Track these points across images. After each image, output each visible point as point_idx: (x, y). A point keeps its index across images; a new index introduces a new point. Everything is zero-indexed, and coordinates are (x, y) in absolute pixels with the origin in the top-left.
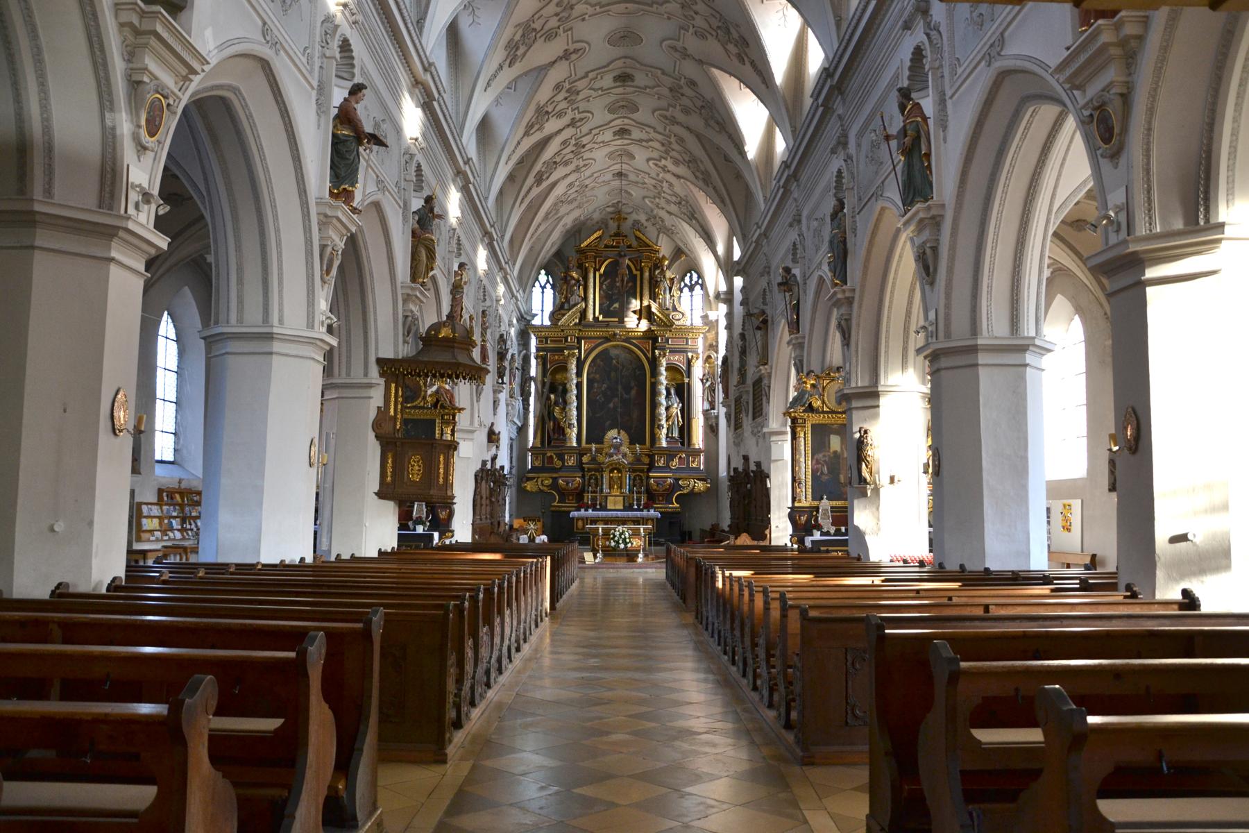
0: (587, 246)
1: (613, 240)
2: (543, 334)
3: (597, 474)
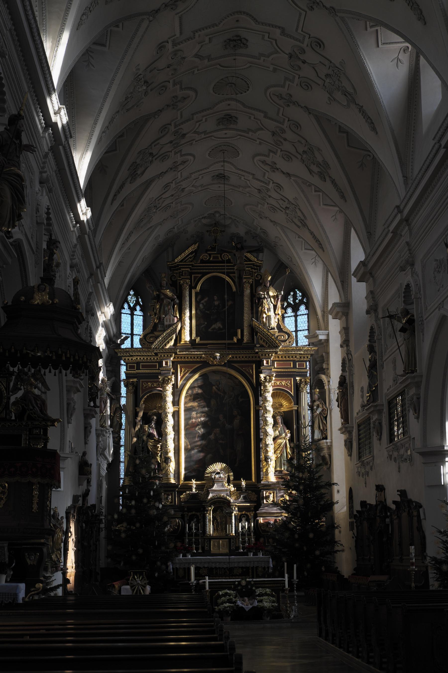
0: (181, 261)
1: (210, 255)
2: (134, 358)
3: (198, 514)
